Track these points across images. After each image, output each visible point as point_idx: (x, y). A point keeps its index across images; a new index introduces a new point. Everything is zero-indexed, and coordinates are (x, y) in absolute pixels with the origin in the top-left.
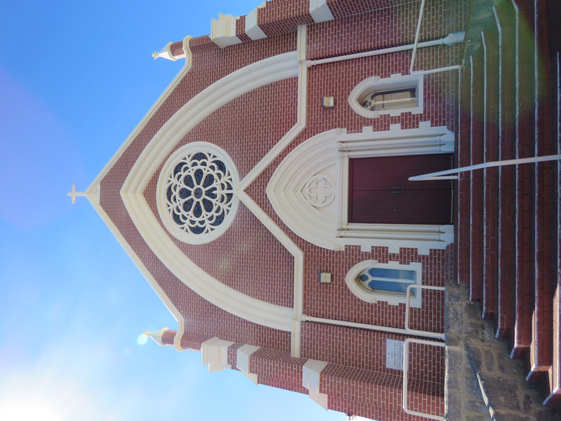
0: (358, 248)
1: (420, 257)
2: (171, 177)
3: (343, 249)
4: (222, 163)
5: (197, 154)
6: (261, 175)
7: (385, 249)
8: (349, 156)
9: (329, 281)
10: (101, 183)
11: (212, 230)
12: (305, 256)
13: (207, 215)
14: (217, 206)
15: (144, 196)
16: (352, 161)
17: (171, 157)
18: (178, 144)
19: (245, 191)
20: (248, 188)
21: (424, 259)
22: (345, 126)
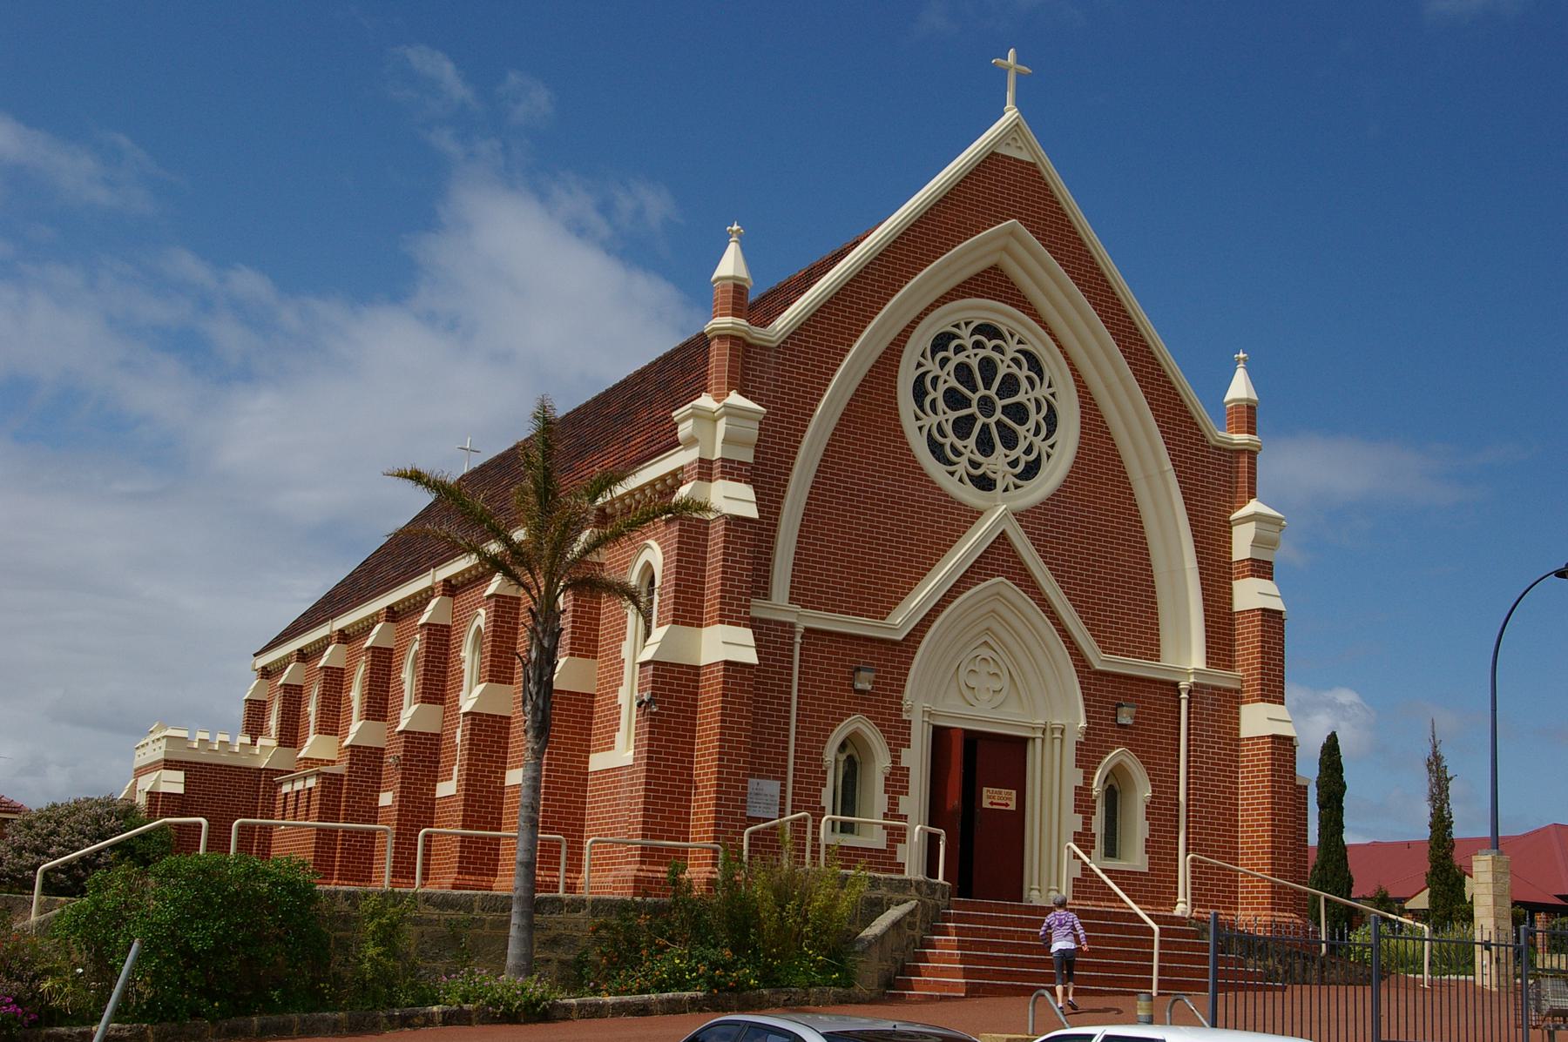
0: (906, 743)
1: (894, 847)
2: (1020, 342)
3: (905, 717)
4: (1036, 474)
5: (1055, 417)
6: (1025, 570)
7: (904, 790)
8: (1034, 739)
9: (859, 686)
10: (1034, 165)
11: (920, 428)
12: (894, 643)
13: (947, 420)
14: (963, 450)
15: (991, 268)
16: (1021, 743)
17: (1057, 350)
18: (1079, 376)
19: (1003, 533)
20: (1005, 539)
21: (891, 852)
22: (1086, 739)
